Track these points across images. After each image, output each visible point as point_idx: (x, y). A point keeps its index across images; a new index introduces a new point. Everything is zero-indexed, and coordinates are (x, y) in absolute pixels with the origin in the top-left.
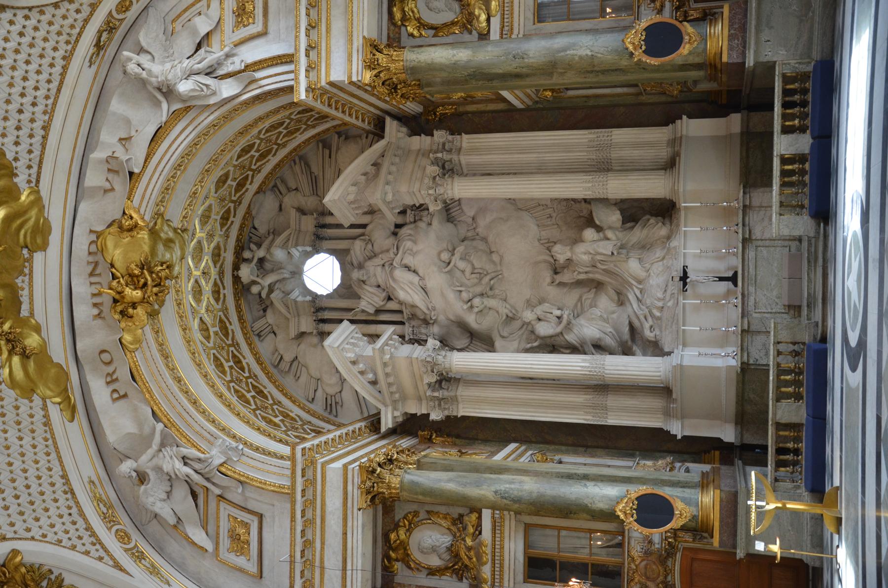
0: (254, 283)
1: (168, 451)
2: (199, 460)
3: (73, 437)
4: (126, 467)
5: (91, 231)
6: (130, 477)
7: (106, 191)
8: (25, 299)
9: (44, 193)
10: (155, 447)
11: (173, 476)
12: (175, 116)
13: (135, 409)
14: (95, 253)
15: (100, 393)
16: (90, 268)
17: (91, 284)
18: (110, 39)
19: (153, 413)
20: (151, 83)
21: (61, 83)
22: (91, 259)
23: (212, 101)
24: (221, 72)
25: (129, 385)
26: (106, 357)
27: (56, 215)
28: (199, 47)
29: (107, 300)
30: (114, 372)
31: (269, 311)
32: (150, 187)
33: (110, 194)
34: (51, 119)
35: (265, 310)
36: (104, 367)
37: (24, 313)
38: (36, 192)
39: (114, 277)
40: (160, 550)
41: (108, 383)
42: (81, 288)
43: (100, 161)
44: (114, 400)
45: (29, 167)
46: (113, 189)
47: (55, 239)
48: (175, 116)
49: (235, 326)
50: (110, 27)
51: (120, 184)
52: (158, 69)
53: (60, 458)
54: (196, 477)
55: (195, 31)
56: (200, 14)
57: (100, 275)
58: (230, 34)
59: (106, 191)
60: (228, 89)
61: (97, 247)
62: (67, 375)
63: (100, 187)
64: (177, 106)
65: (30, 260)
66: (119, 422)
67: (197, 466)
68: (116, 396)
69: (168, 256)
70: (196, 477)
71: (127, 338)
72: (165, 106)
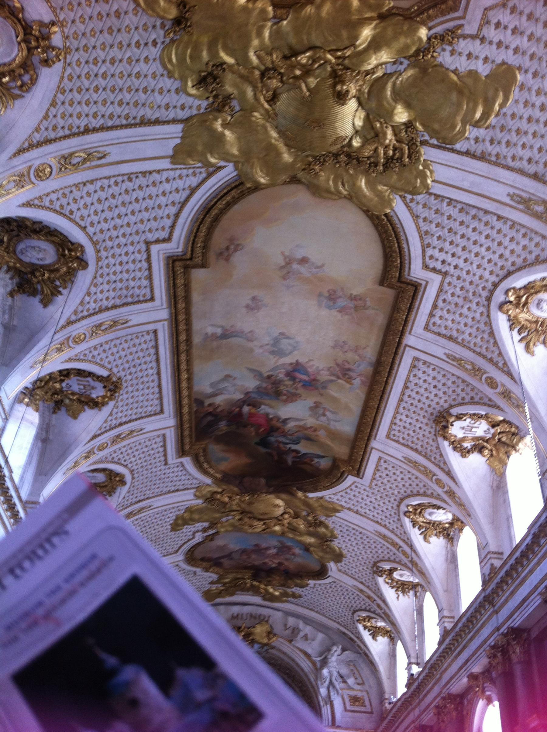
5: (269, 617)
12: (314, 663)
20: (329, 654)
23: (319, 682)
24: (331, 688)
28: (342, 677)
32: (286, 647)
39: (249, 628)
42: (246, 610)
43: (298, 625)
48: (314, 663)
52: (333, 659)
55: (349, 677)
56: (356, 679)
58: (346, 693)
60: (323, 691)
64: (318, 665)
65: (258, 595)
72: (319, 659)
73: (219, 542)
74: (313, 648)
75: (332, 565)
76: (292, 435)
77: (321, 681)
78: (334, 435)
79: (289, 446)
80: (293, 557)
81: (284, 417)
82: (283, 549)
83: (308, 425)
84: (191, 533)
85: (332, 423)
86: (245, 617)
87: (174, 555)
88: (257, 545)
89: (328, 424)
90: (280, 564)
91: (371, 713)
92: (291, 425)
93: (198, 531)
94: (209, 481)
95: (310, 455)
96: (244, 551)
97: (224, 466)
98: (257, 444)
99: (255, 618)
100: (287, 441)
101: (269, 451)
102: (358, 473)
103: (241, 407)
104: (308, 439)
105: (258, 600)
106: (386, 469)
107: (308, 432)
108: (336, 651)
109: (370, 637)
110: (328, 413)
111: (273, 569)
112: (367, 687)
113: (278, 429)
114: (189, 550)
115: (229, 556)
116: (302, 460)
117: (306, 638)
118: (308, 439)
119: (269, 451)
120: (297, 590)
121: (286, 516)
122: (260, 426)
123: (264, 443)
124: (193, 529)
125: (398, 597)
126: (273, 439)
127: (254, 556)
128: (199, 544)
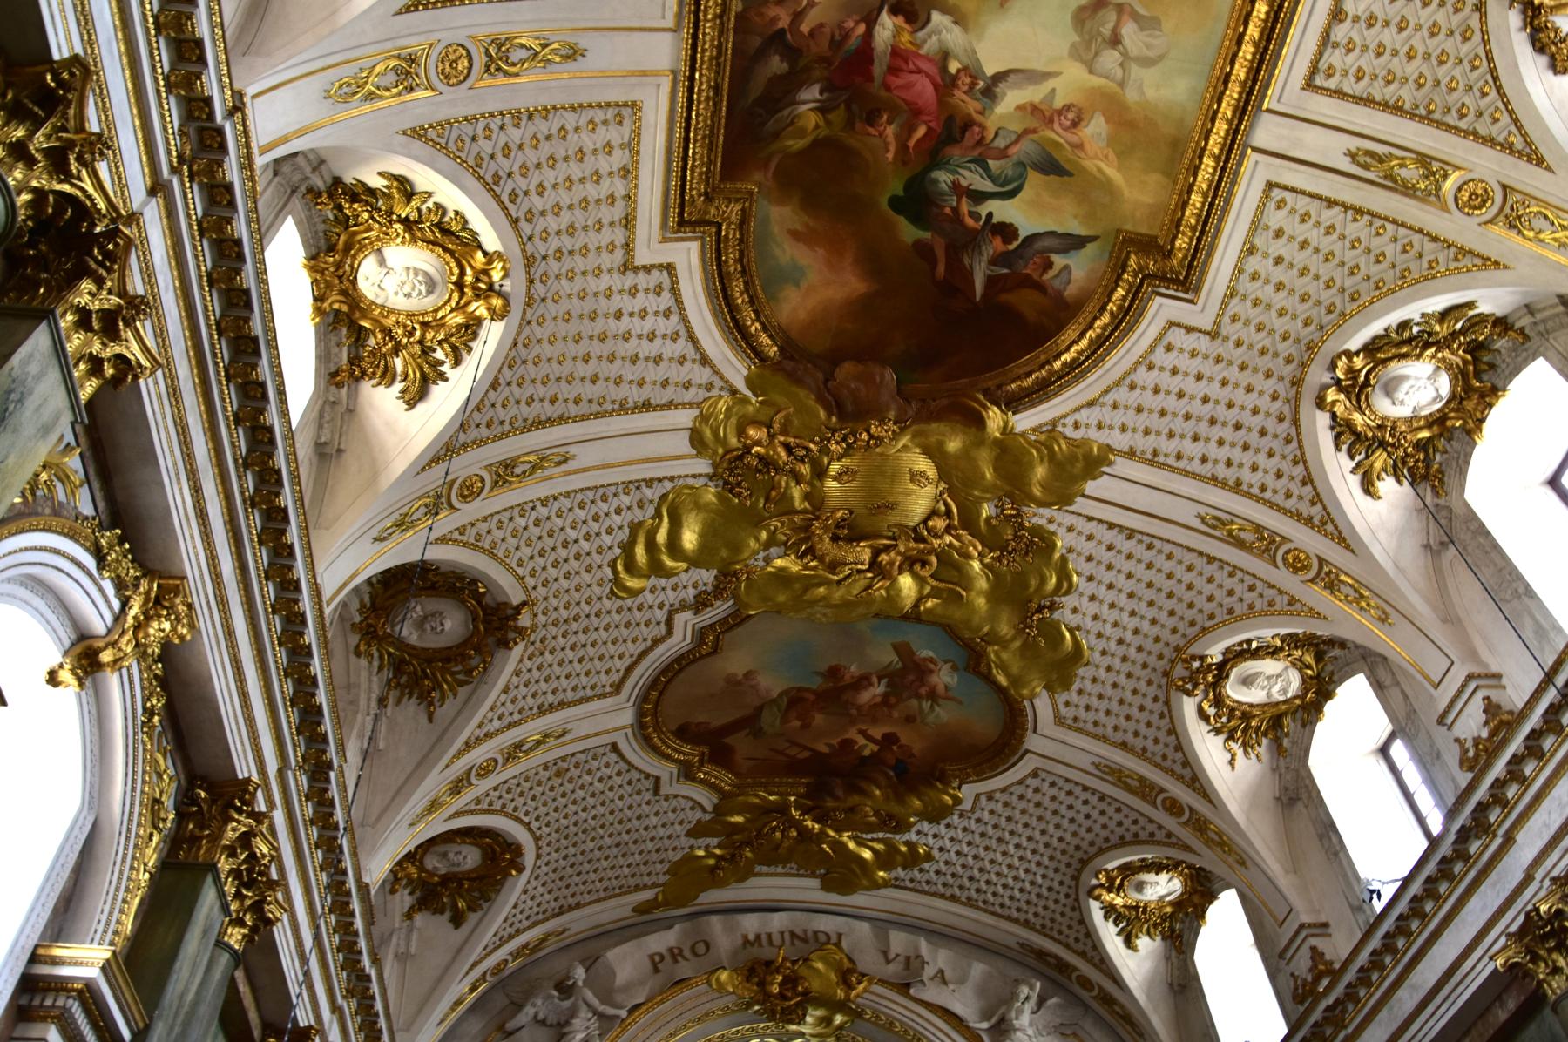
1: (594, 1024)
3: (618, 909)
4: (580, 973)
5: (840, 936)
6: (569, 978)
7: (885, 953)
8: (772, 869)
9: (883, 892)
10: (602, 1008)
11: (566, 1030)
13: (641, 983)
14: (817, 940)
15: (660, 942)
16: (800, 933)
17: (782, 933)
18: (1049, 964)
19: (638, 1006)
20: (1009, 1010)
21: (1000, 916)
22: (810, 934)
25: (668, 977)
26: (701, 948)
27: (859, 899)
29: (766, 953)
30: (685, 959)
32: (896, 1007)
33: (882, 960)
34: (962, 903)
36: (689, 944)
37: (758, 869)
38: (886, 884)
39: (794, 962)
40: (473, 1009)
41: (671, 950)
42: (778, 922)
43: (917, 948)
44: (651, 957)
45: (912, 881)
46: (888, 962)
47: (834, 898)
50: (1063, 967)
51: (893, 970)
53: (599, 900)
57: (793, 944)
59: (885, 953)
61: (820, 942)
62: (684, 906)
63: (888, 946)
65: (813, 875)
68: (657, 959)
69: (809, 1019)
71: (724, 976)
72: (985, 1025)
73: (735, 661)
74: (963, 1004)
75: (1043, 706)
76: (1002, 154)
78: (1131, 128)
79: (984, 210)
80: (926, 705)
81: (990, 70)
82: (909, 676)
83: (1058, 103)
84: (661, 615)
85: (1135, 71)
86: (777, 940)
87: (609, 700)
88: (834, 672)
89: (1122, 84)
90: (890, 739)
92: (1011, 99)
93: (683, 606)
94: (736, 370)
95: (1047, 242)
96: (795, 701)
97: (794, 306)
98: (895, 203)
99: (805, 940)
100: (988, 186)
101: (926, 235)
102: (1186, 281)
103: (871, 21)
104: (1051, 166)
105: (807, 889)
106: (1279, 233)
107: (1055, 134)
108: (1027, 998)
109: (1119, 941)
110: (1129, 31)
111: (864, 761)
113: (969, 124)
114: (654, 684)
115: (749, 723)
116: (1024, 257)
117: (941, 976)
118: (1051, 166)
119: (927, 235)
120: (922, 834)
121: (939, 524)
122: (916, 112)
123: (917, 201)
124: (672, 597)
125: (1232, 763)
126: (943, 178)
127: (819, 719)
128: (680, 664)
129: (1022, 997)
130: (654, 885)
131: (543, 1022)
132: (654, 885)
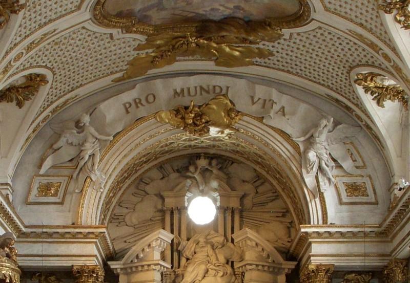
0: (196, 168)
1: (97, 145)
2: (93, 165)
7: (252, 98)
12: (295, 146)
15: (128, 97)
23: (304, 171)
28: (334, 160)
31: (176, 175)
35: (178, 171)
46: (253, 103)
48: (295, 146)
49: (167, 156)
51: (255, 109)
52: (322, 138)
54: (82, 163)
59: (252, 98)
60: (309, 180)
66: (111, 110)
67: (90, 164)
70: (82, 163)
74: (292, 127)
77: (306, 168)
91: (376, 203)
112: (369, 171)
129: (323, 126)
130: (121, 71)
131: (71, 144)
132: (121, 71)
